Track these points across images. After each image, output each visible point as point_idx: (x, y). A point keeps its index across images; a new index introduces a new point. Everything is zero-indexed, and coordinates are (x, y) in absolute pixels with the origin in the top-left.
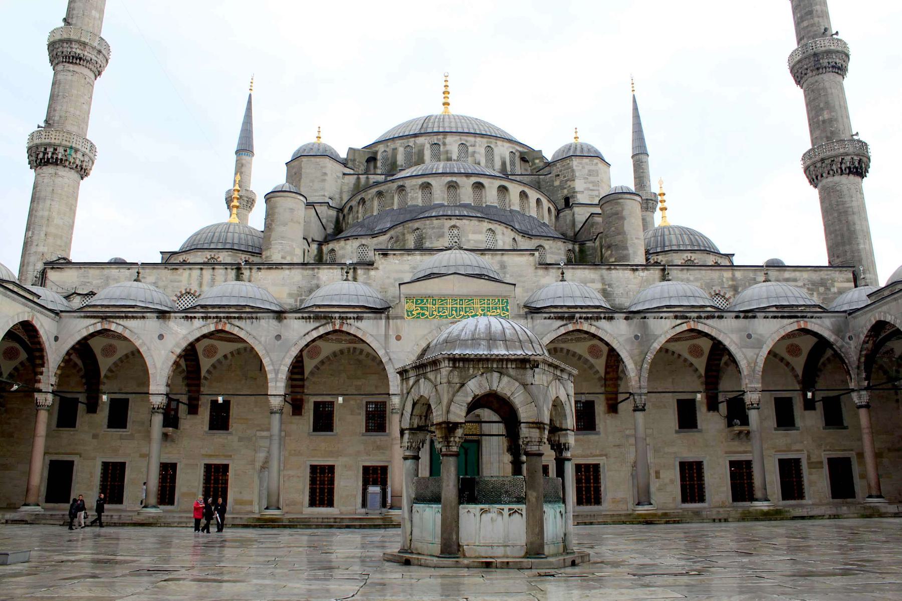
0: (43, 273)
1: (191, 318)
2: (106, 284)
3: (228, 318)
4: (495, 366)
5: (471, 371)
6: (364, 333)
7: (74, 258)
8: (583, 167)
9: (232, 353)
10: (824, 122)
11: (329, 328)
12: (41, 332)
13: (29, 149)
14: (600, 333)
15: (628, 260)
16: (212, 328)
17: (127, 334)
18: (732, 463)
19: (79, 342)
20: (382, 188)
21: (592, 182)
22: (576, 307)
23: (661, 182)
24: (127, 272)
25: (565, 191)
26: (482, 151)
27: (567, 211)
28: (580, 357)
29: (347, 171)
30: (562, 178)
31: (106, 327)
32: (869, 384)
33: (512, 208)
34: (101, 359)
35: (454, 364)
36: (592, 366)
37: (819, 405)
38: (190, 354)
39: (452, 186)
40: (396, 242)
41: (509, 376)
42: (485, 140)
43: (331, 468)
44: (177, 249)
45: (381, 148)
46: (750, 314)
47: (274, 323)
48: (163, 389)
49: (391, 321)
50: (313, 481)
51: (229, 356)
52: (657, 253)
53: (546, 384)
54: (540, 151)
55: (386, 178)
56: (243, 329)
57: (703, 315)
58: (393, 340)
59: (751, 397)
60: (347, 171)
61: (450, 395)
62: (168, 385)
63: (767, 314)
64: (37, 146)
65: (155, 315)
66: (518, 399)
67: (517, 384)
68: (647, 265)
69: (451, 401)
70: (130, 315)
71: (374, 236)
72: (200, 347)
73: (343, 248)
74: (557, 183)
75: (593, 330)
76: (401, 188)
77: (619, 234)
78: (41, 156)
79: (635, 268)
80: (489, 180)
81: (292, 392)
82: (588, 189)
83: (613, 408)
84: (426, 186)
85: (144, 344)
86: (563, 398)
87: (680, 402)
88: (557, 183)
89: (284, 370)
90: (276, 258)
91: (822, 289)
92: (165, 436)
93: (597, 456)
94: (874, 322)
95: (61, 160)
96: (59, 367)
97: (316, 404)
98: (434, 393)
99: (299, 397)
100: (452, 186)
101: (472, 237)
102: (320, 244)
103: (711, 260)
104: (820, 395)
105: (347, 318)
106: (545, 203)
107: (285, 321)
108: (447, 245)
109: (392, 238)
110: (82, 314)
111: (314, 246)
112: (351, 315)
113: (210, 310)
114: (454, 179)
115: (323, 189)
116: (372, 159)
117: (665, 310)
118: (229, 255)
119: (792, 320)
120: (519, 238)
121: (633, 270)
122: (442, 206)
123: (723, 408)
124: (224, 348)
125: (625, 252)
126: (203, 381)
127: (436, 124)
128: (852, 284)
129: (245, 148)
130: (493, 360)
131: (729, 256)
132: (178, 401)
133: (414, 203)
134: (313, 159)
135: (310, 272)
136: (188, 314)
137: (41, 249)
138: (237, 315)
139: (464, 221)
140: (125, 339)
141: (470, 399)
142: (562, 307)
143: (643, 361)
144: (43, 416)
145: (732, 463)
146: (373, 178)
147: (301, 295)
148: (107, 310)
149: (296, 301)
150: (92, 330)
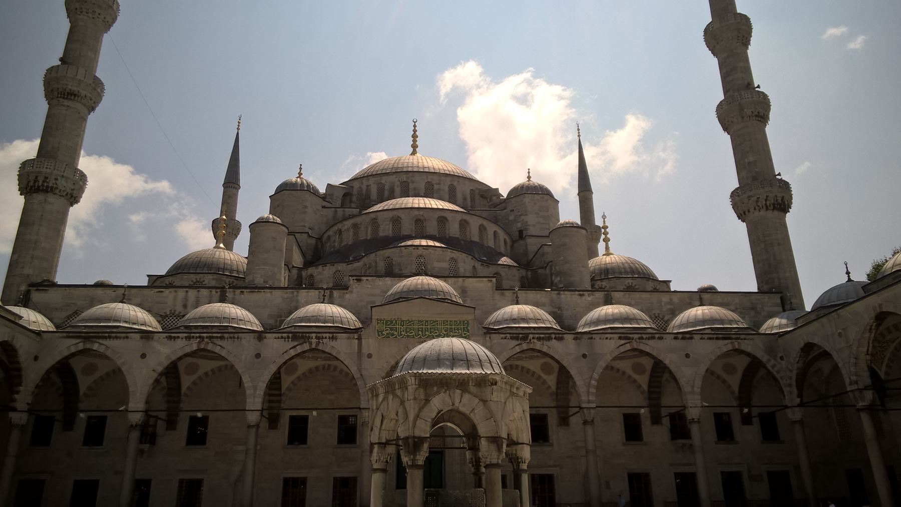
0: (27, 294)
1: (175, 338)
2: (92, 305)
3: (210, 338)
5: (435, 389)
6: (339, 352)
7: (60, 279)
9: (213, 370)
10: (749, 163)
11: (306, 347)
14: (551, 353)
16: (195, 347)
17: (109, 353)
18: (677, 475)
19: (59, 362)
20: (358, 220)
23: (604, 217)
24: (113, 294)
25: (519, 225)
26: (447, 188)
27: (521, 242)
28: (534, 373)
31: (88, 346)
32: (801, 401)
33: (473, 239)
36: (544, 382)
37: (756, 421)
38: (172, 372)
40: (369, 268)
41: (470, 393)
42: (448, 179)
43: (303, 481)
44: (163, 273)
45: (356, 185)
46: (688, 336)
48: (141, 406)
49: (363, 341)
50: (285, 494)
51: (210, 373)
55: (360, 212)
56: (225, 348)
57: (644, 336)
58: (365, 358)
59: (693, 413)
61: (417, 409)
62: (147, 402)
63: (704, 336)
65: (138, 336)
67: (477, 401)
68: (594, 289)
69: (417, 416)
70: (113, 335)
71: (349, 263)
72: (182, 366)
75: (545, 349)
78: (31, 184)
79: (582, 292)
83: (564, 421)
87: (626, 417)
88: (512, 218)
89: (262, 386)
90: (259, 281)
91: (752, 313)
92: (141, 452)
93: (550, 466)
94: (803, 344)
95: (52, 188)
96: (37, 387)
97: (292, 418)
99: (275, 411)
101: (436, 265)
103: (650, 286)
104: (755, 412)
106: (502, 235)
108: (414, 271)
110: (65, 335)
111: (295, 271)
114: (421, 213)
116: (345, 195)
117: (610, 331)
118: (213, 279)
119: (727, 341)
120: (478, 265)
121: (580, 295)
123: (666, 421)
124: (206, 366)
126: (183, 398)
128: (780, 309)
129: (232, 181)
131: (667, 283)
132: (157, 417)
133: (386, 234)
137: (27, 271)
138: (219, 335)
140: (106, 357)
141: (434, 415)
143: (591, 378)
144: (15, 435)
145: (677, 475)
146: (348, 211)
149: (276, 321)
150: (73, 350)
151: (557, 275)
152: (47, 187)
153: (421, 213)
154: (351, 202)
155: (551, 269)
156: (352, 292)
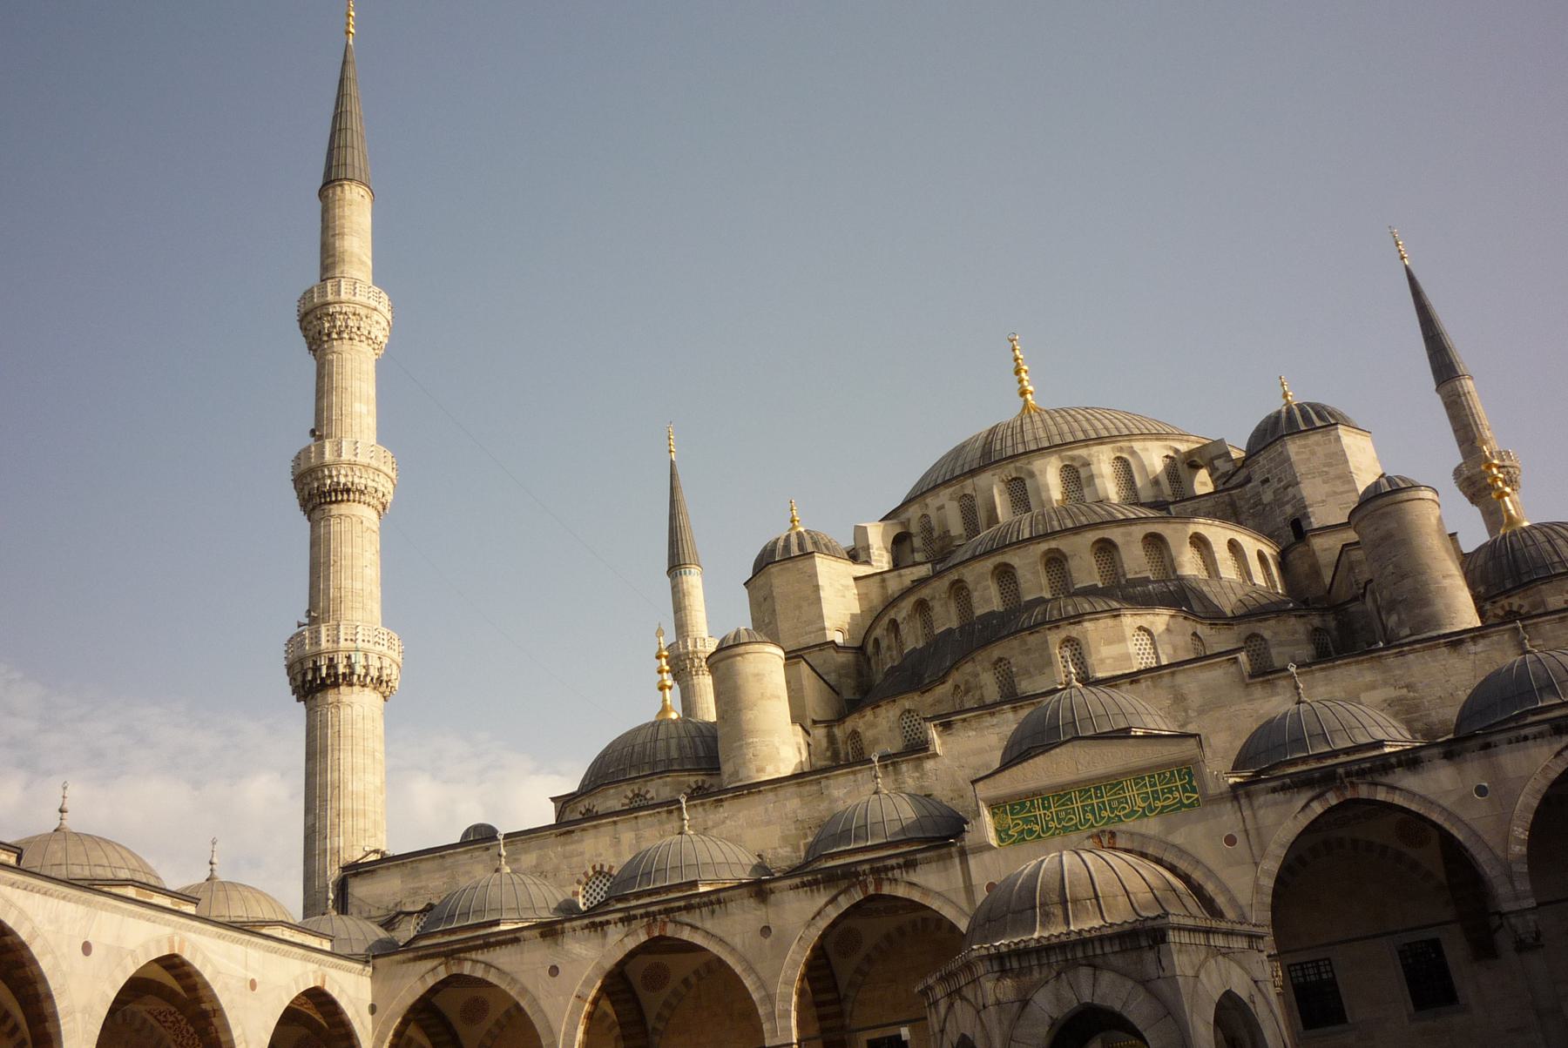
0: (342, 887)
1: (602, 924)
3: (667, 912)
4: (1080, 954)
5: (1036, 975)
6: (926, 891)
8: (1313, 453)
9: (696, 972)
11: (858, 896)
12: (343, 1003)
13: (290, 668)
14: (1398, 799)
15: (1439, 626)
16: (643, 938)
17: (492, 978)
20: (925, 593)
21: (1339, 477)
22: (1334, 754)
25: (1289, 509)
27: (1301, 548)
29: (862, 570)
30: (1275, 484)
31: (455, 970)
34: (462, 1029)
35: (1002, 964)
39: (1055, 561)
40: (967, 692)
44: (573, 787)
47: (752, 902)
52: (1507, 593)
53: (1190, 972)
54: (1221, 441)
60: (862, 570)
64: (302, 660)
65: (536, 932)
66: (1138, 1010)
67: (1130, 984)
69: (1009, 1040)
72: (635, 974)
73: (872, 725)
74: (1268, 497)
75: (1381, 795)
76: (959, 590)
77: (1404, 576)
80: (1121, 530)
81: (823, 1031)
82: (1335, 493)
84: (1005, 574)
85: (524, 991)
86: (1242, 989)
88: (1268, 497)
98: (979, 1028)
100: (1055, 561)
102: (829, 724)
105: (887, 869)
106: (1251, 545)
107: (772, 897)
109: (957, 687)
110: (411, 955)
111: (820, 732)
112: (893, 862)
113: (634, 903)
114: (1053, 544)
115: (821, 617)
118: (666, 784)
120: (1203, 630)
122: (1041, 601)
124: (680, 967)
125: (1426, 611)
127: (1009, 443)
130: (1074, 944)
134: (790, 565)
135: (815, 788)
136: (595, 920)
138: (682, 903)
139: (1087, 624)
141: (1043, 1030)
142: (1304, 760)
146: (911, 574)
147: (806, 836)
148: (454, 938)
149: (796, 849)
150: (431, 982)
151: (1389, 613)
152: (336, 675)
153: (1053, 544)
154: (913, 551)
155: (1375, 601)
156: (935, 755)
